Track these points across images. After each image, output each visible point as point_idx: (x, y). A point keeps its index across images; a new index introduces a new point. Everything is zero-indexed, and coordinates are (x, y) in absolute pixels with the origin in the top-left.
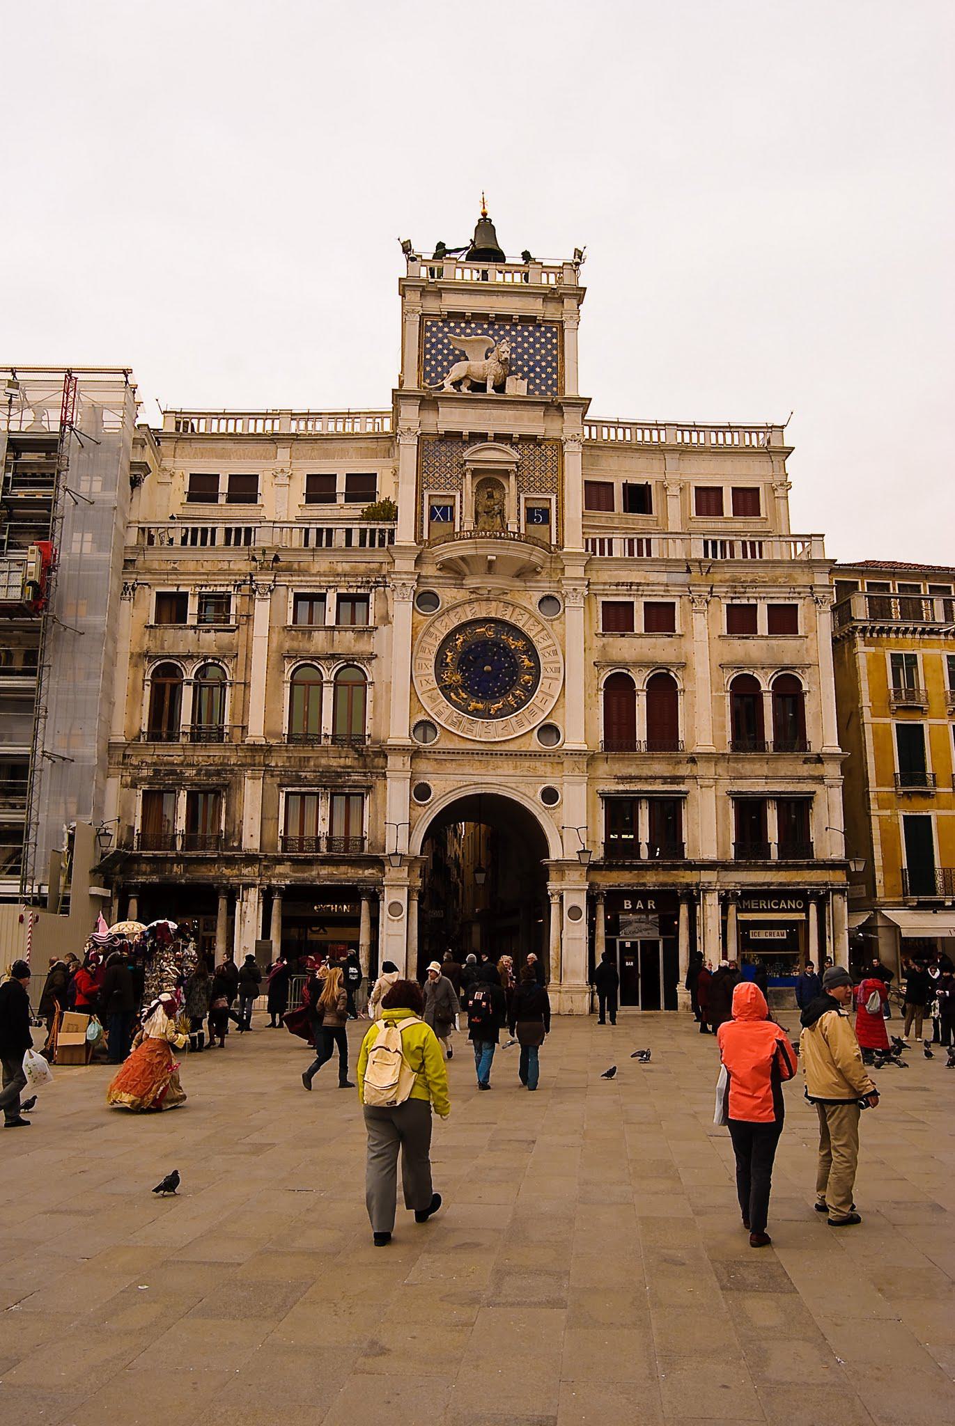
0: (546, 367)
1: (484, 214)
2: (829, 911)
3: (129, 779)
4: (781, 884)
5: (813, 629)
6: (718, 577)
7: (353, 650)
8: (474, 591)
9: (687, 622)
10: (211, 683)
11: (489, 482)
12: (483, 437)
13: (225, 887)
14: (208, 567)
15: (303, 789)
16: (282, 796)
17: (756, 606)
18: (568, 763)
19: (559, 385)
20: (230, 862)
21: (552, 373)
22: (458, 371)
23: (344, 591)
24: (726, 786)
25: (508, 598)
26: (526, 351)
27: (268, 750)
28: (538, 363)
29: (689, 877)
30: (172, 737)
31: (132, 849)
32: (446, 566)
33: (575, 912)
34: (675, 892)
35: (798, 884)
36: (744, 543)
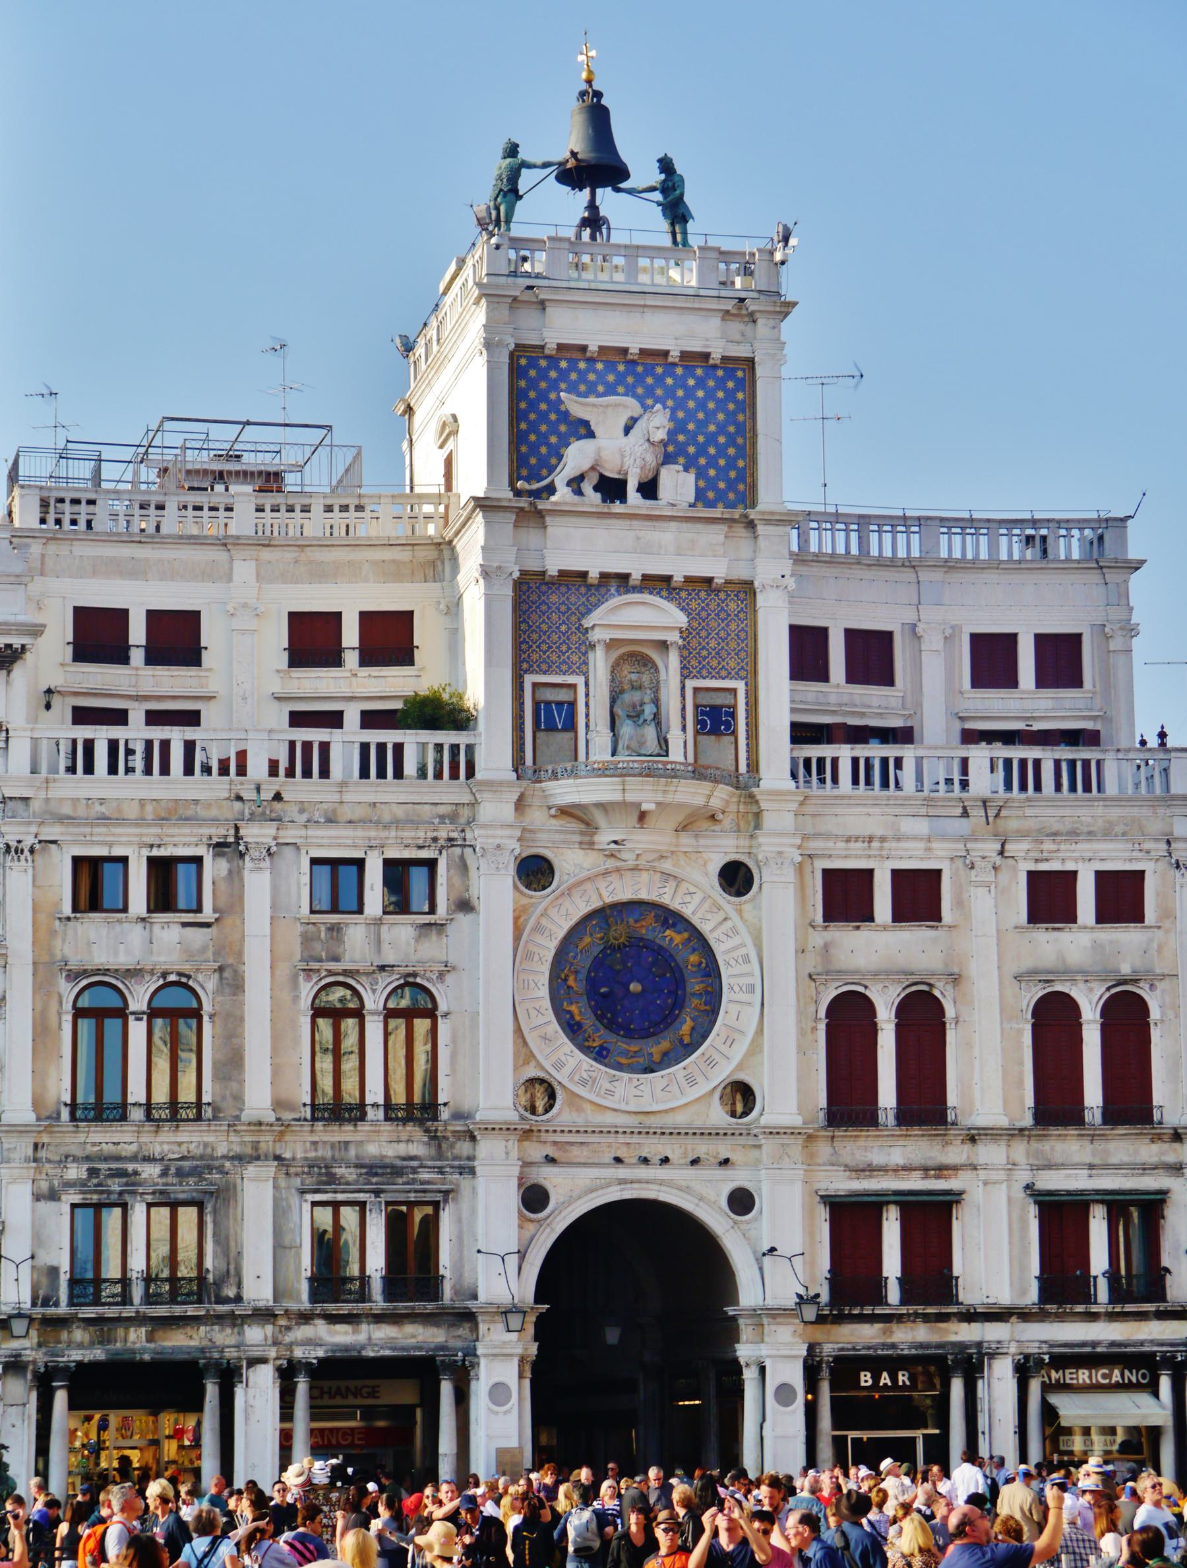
1: (589, 82)
3: (44, 1186)
4: (1113, 1344)
6: (1013, 824)
7: (414, 958)
9: (960, 903)
10: (177, 1013)
11: (635, 658)
13: (218, 1363)
15: (340, 1197)
16: (307, 1207)
17: (1075, 873)
18: (769, 1146)
20: (219, 1319)
21: (735, 459)
22: (577, 456)
26: (691, 416)
27: (283, 1128)
28: (711, 439)
29: (966, 1333)
30: (121, 1112)
31: (57, 1304)
32: (565, 812)
34: (943, 1358)
35: (1142, 1343)
36: (1057, 763)
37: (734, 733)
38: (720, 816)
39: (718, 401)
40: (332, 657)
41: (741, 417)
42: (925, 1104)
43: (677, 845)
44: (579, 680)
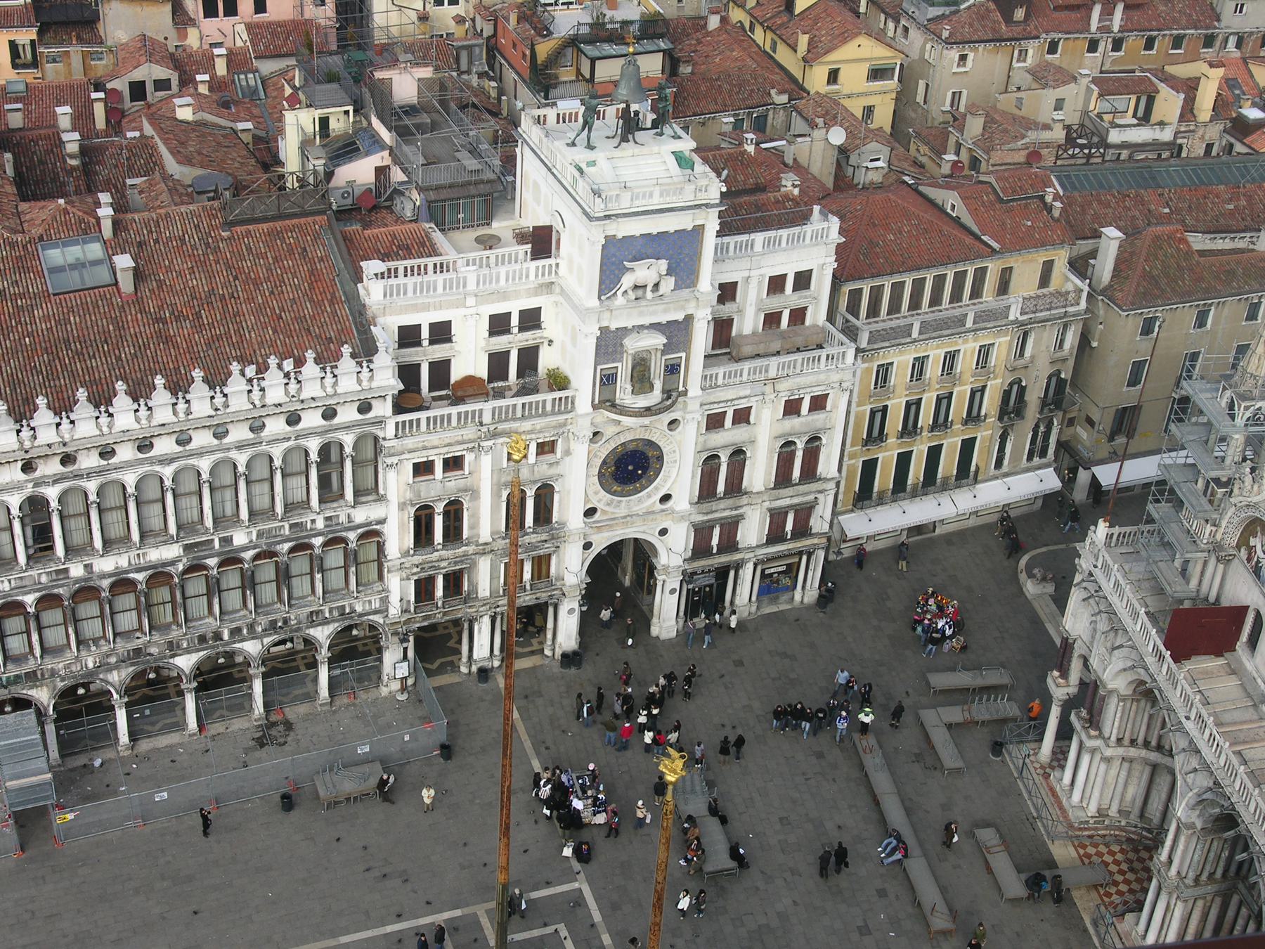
2: (813, 557)
5: (835, 406)
9: (757, 417)
12: (642, 327)
14: (447, 441)
23: (540, 441)
24: (767, 504)
33: (672, 591)
40: (507, 331)
42: (735, 487)
44: (619, 365)
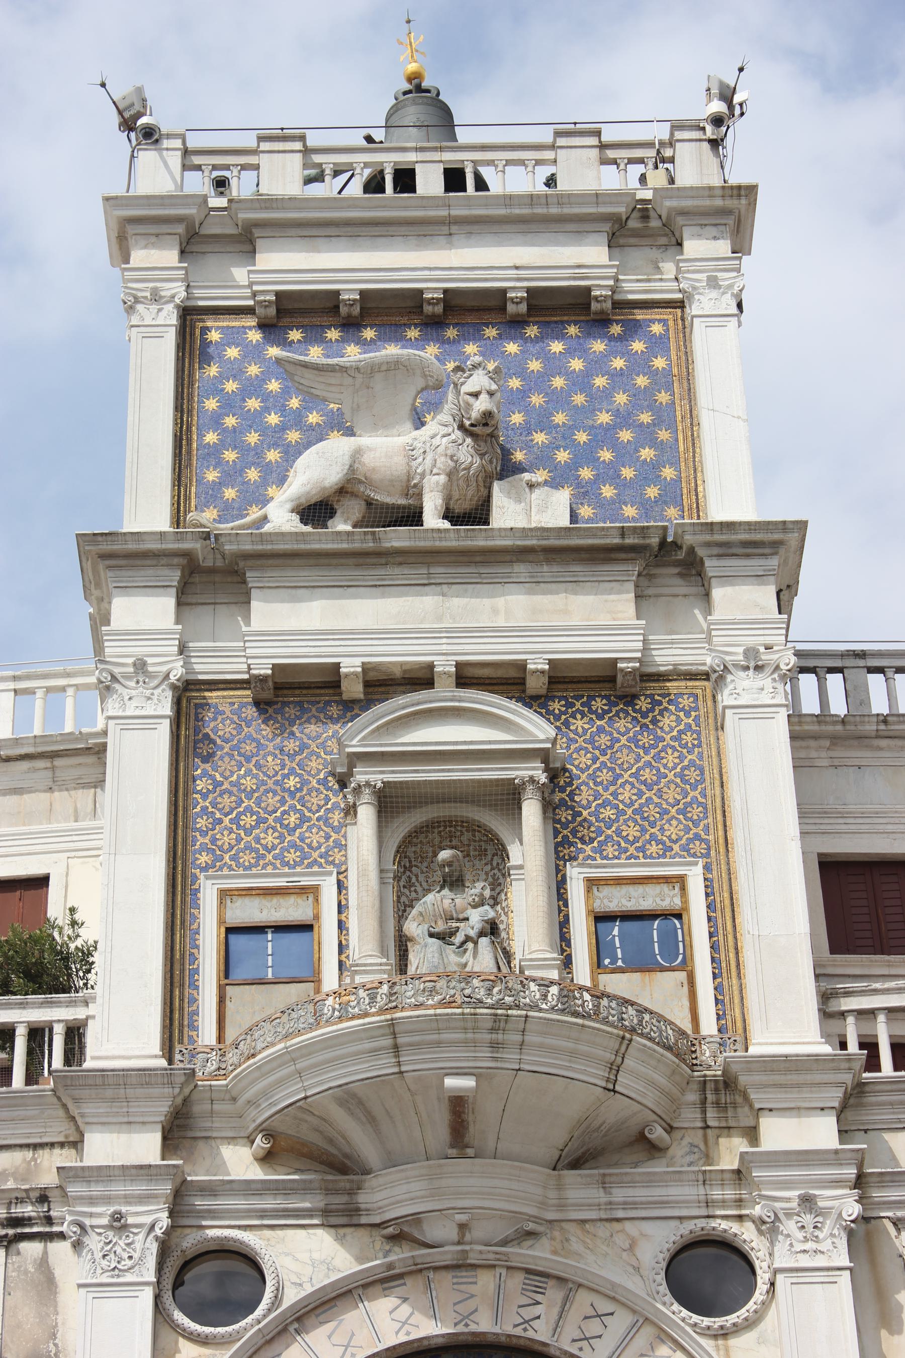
0: (637, 445)
8: (400, 1234)
19: (685, 491)
21: (655, 466)
25: (539, 1254)
26: (558, 400)
37: (687, 966)
38: (657, 1133)
39: (616, 376)
41: (663, 397)
43: (561, 1207)
